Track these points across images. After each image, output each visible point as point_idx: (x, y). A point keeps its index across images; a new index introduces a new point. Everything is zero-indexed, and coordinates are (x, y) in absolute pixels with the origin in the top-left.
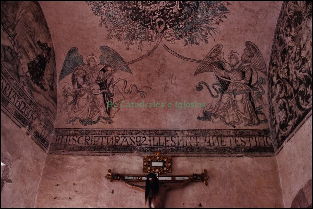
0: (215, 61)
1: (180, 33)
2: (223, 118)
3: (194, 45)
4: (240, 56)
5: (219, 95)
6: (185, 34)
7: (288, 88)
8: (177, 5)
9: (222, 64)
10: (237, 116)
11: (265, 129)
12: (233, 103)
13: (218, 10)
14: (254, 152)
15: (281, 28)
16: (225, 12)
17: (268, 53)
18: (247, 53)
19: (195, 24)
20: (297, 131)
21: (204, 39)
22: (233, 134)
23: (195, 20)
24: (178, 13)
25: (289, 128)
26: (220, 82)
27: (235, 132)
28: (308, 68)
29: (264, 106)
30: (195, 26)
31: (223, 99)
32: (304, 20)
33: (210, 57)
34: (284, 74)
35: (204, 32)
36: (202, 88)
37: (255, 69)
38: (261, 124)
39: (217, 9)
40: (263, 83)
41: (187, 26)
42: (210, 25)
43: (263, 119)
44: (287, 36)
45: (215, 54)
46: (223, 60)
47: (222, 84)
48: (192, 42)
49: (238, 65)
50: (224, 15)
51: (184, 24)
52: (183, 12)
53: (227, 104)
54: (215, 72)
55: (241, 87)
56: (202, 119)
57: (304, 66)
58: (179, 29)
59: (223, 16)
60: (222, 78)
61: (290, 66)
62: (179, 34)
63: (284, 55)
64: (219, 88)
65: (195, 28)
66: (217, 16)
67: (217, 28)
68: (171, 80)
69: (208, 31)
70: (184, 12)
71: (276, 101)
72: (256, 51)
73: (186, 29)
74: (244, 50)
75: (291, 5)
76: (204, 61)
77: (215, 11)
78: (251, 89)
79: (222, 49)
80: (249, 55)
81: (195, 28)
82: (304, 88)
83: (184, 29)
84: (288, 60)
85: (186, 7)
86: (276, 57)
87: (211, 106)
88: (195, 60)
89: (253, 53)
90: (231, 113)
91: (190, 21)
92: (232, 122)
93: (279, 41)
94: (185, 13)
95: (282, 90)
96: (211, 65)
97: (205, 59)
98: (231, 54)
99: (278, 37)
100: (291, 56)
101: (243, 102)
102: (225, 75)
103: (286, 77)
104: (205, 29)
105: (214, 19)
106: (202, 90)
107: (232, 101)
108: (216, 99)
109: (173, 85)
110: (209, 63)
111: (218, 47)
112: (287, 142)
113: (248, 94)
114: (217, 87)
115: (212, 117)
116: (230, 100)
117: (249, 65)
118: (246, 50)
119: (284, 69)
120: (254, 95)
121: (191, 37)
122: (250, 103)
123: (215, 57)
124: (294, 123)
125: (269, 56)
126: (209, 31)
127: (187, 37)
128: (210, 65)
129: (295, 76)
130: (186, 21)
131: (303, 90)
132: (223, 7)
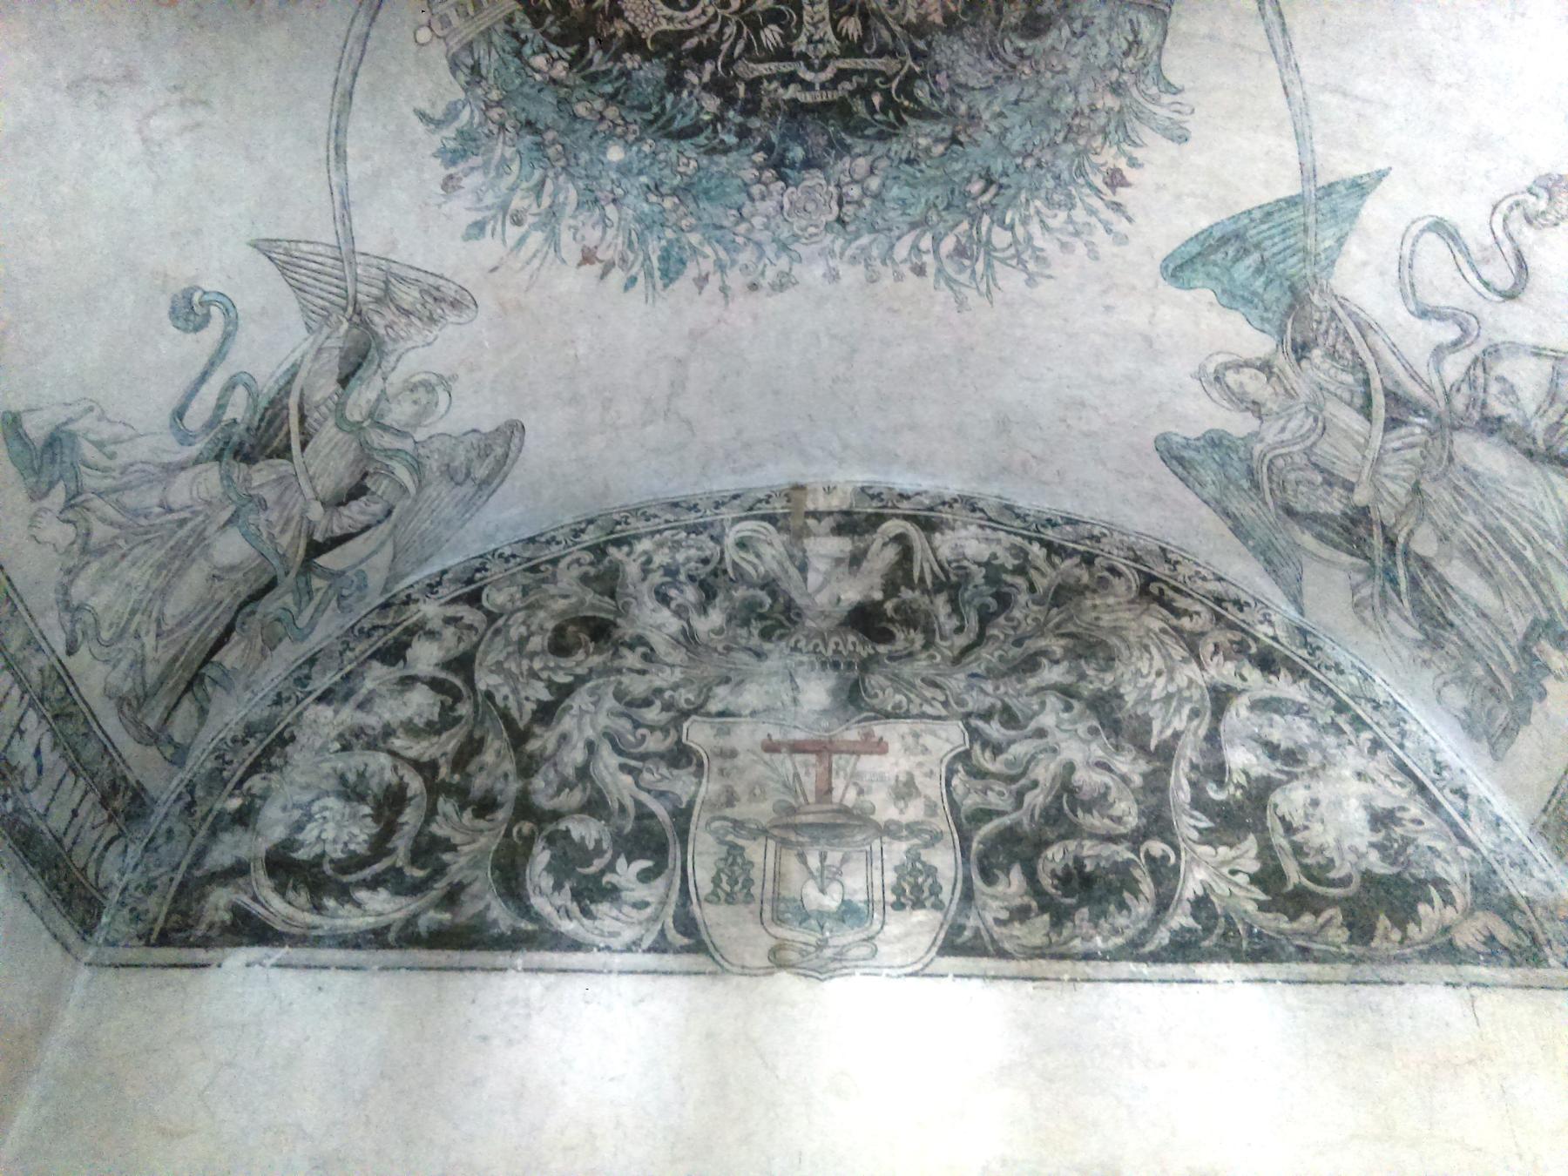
0: (376, 319)
1: (494, 65)
2: (84, 550)
3: (436, 171)
4: (441, 427)
5: (198, 446)
6: (495, 95)
7: (488, 757)
8: (670, 19)
9: (371, 362)
10: (133, 612)
11: (143, 789)
12: (190, 542)
13: (664, 243)
14: (33, 865)
15: (645, 545)
16: (657, 274)
17: (490, 537)
18: (461, 450)
19: (567, 141)
20: (409, 968)
21: (488, 214)
22: (35, 677)
23: (588, 131)
24: (620, 28)
25: (351, 920)
26: (272, 402)
27: (54, 675)
28: (685, 799)
29: (239, 687)
30: (554, 142)
31: (183, 478)
32: (795, 649)
33: (387, 282)
34: (515, 691)
35: (526, 203)
36: (196, 329)
37: (395, 526)
38: (152, 751)
39: (669, 234)
40: (344, 603)
41: (549, 97)
42: (572, 222)
43: (177, 738)
44: (664, 599)
45: (413, 304)
46: (393, 359)
47: (263, 424)
48: (454, 151)
49: (388, 441)
50: (641, 279)
51: (554, 81)
52: (631, 61)
53: (170, 517)
54: (316, 347)
55: (288, 522)
56: (17, 447)
57: (664, 771)
58: (518, 54)
59: (634, 271)
60: (293, 402)
61: (580, 700)
62: (489, 63)
63: (584, 637)
64: (235, 421)
65: (540, 146)
66: (630, 244)
67: (564, 261)
68: (167, 105)
69: (536, 219)
70: (629, 65)
71: (341, 736)
72: (485, 482)
73: (526, 96)
74: (474, 431)
75: (770, 544)
76: (360, 259)
77: (657, 228)
78: (293, 574)
79: (450, 330)
80: (456, 463)
81: (540, 146)
82: (598, 842)
83: (522, 85)
84: (591, 670)
85: (662, 74)
86: (525, 591)
87: (117, 441)
88: (345, 205)
89: (468, 474)
90: (134, 574)
91: (581, 109)
92: (88, 618)
93: (592, 564)
94: (625, 73)
95: (433, 729)
96: (345, 309)
97: (375, 262)
98: (434, 380)
99: (599, 550)
100: (626, 680)
101: (217, 584)
102: (317, 407)
103: (515, 713)
104: (546, 201)
105: (611, 232)
106: (186, 330)
107: (193, 530)
108: (169, 441)
109: (140, 131)
110: (351, 291)
111: (455, 304)
112: (279, 966)
113: (265, 579)
114: (238, 408)
115: (58, 496)
116: (195, 513)
117: (405, 490)
118: (473, 438)
119: (534, 675)
120: (271, 605)
121: (485, 140)
122: (226, 620)
123: (398, 308)
124: (412, 920)
125: (476, 549)
126: (534, 227)
127: (477, 113)
128: (343, 302)
129: (577, 755)
130: (572, 88)
131: (591, 846)
132: (682, 262)
